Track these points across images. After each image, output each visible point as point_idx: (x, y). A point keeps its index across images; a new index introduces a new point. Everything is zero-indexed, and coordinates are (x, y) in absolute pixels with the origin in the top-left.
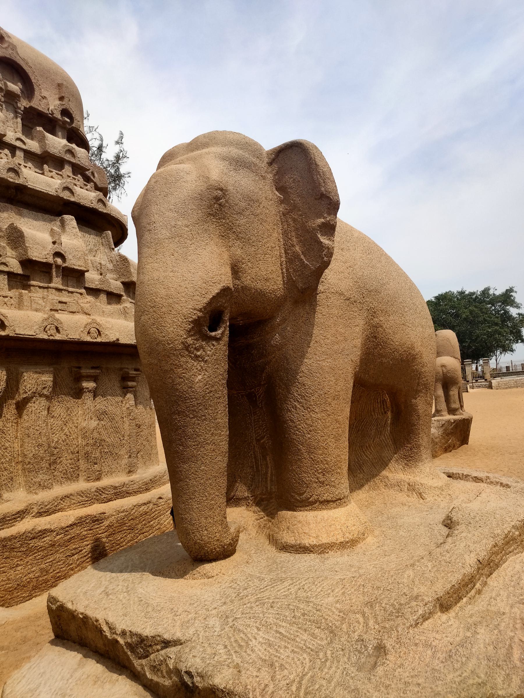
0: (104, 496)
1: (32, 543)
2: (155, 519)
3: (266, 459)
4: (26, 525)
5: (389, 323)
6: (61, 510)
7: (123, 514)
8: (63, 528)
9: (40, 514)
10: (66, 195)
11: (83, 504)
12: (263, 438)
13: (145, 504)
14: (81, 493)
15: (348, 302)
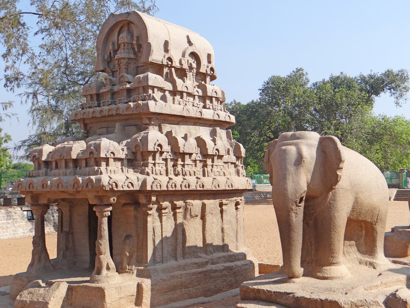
0: (231, 259)
1: (213, 274)
2: (249, 272)
3: (311, 247)
4: (210, 267)
5: (363, 198)
6: (218, 263)
7: (239, 268)
8: (220, 270)
9: (212, 264)
10: (216, 118)
11: (225, 262)
12: (311, 239)
13: (246, 265)
14: (224, 257)
15: (346, 191)
